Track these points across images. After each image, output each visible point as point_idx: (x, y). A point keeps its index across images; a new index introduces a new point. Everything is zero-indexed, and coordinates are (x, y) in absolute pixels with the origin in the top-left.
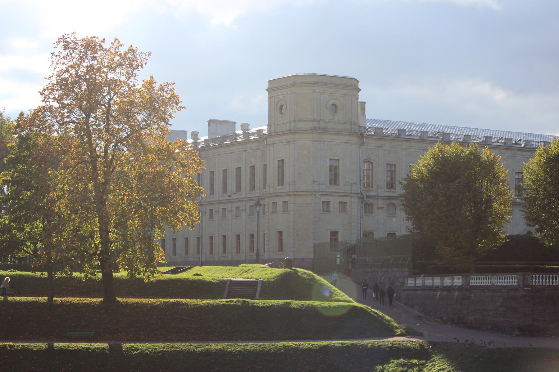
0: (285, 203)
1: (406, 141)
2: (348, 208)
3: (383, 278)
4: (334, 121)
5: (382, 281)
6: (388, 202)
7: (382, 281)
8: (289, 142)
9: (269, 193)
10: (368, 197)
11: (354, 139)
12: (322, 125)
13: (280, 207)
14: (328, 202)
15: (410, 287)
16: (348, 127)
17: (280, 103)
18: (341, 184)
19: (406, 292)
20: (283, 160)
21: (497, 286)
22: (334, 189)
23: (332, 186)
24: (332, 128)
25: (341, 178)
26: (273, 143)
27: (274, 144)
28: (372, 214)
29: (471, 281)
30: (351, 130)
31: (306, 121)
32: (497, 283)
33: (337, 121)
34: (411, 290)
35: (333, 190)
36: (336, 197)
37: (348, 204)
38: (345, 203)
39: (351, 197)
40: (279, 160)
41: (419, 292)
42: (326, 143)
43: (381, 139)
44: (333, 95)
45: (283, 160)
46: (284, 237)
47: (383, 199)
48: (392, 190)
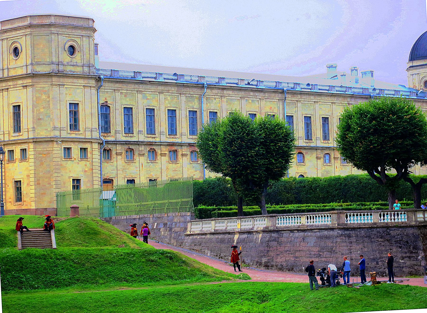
0: (24, 151)
1: (142, 83)
2: (89, 155)
3: (156, 224)
4: (72, 63)
5: (155, 227)
6: (127, 147)
7: (155, 227)
8: (26, 86)
9: (4, 141)
10: (107, 142)
11: (93, 82)
12: (61, 68)
13: (17, 154)
14: (69, 149)
15: (193, 231)
16: (86, 69)
17: (13, 46)
18: (81, 129)
19: (191, 237)
20: (19, 106)
21: (307, 226)
22: (73, 135)
23: (72, 132)
24: (71, 71)
25: (81, 122)
26: (7, 87)
27: (8, 89)
28: (111, 160)
29: (277, 222)
30: (89, 73)
31: (44, 64)
32: (308, 222)
33: (75, 64)
34: (198, 234)
35: (73, 136)
36: (77, 143)
37: (89, 150)
38: (85, 149)
39: (92, 142)
40: (14, 106)
41: (208, 236)
42: (65, 86)
43: (117, 82)
44: (71, 36)
45: (19, 106)
46: (24, 187)
47: (121, 144)
48: (130, 135)
